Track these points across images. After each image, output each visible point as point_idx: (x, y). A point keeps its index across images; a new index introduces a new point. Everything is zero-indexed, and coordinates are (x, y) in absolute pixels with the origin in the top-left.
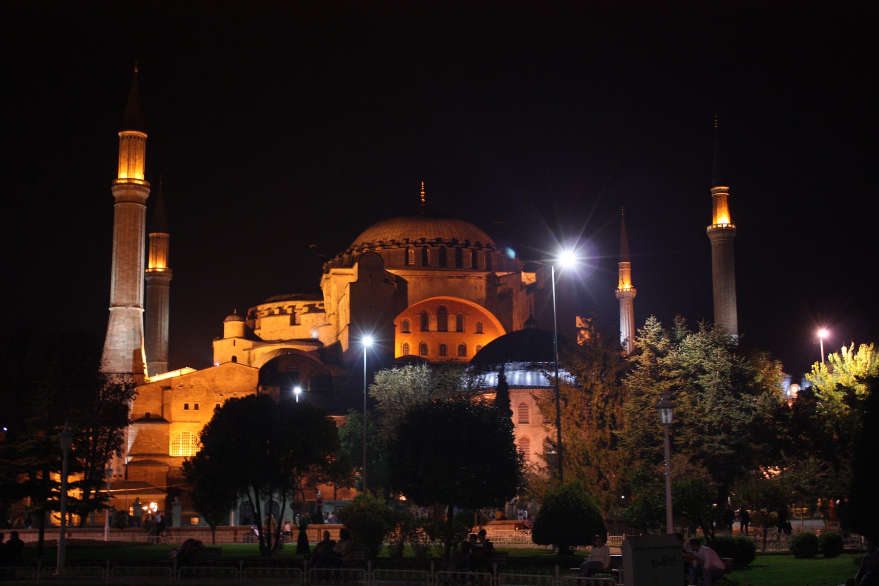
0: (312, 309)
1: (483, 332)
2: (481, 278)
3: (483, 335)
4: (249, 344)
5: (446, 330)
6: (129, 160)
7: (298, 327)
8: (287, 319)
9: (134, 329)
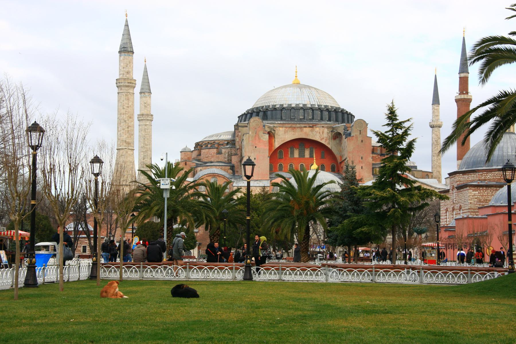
8: (215, 150)
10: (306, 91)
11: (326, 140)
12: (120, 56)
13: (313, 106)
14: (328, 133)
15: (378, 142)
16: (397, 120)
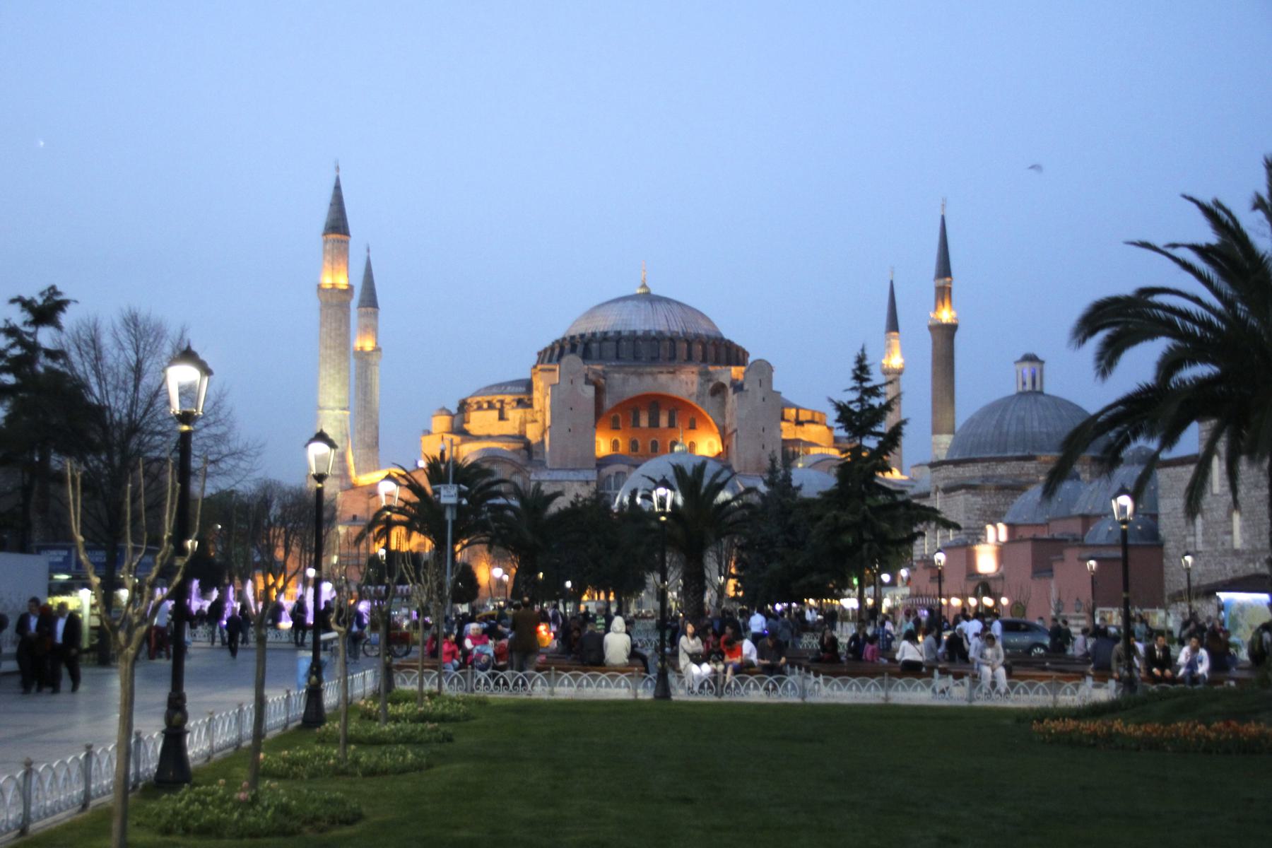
0: (520, 403)
1: (697, 426)
2: (693, 372)
3: (695, 431)
4: (457, 439)
5: (657, 425)
6: (332, 264)
7: (507, 422)
8: (495, 414)
9: (341, 432)
10: (661, 308)
11: (698, 397)
12: (326, 242)
13: (675, 334)
14: (701, 385)
15: (838, 421)
16: (868, 380)
